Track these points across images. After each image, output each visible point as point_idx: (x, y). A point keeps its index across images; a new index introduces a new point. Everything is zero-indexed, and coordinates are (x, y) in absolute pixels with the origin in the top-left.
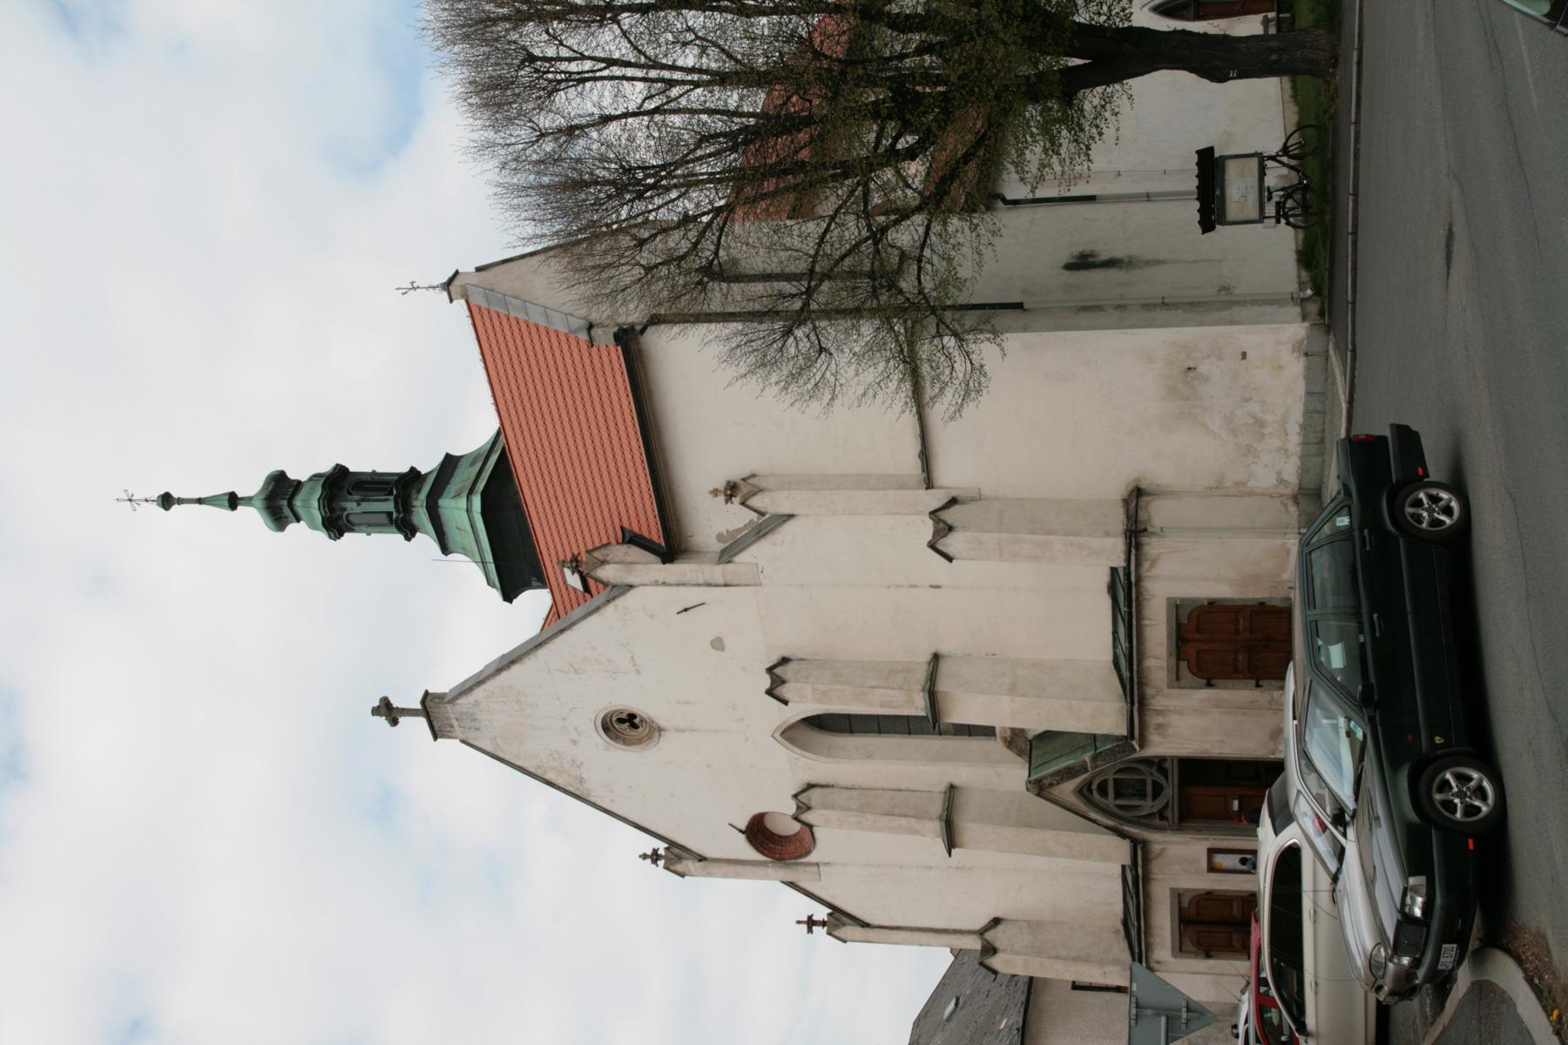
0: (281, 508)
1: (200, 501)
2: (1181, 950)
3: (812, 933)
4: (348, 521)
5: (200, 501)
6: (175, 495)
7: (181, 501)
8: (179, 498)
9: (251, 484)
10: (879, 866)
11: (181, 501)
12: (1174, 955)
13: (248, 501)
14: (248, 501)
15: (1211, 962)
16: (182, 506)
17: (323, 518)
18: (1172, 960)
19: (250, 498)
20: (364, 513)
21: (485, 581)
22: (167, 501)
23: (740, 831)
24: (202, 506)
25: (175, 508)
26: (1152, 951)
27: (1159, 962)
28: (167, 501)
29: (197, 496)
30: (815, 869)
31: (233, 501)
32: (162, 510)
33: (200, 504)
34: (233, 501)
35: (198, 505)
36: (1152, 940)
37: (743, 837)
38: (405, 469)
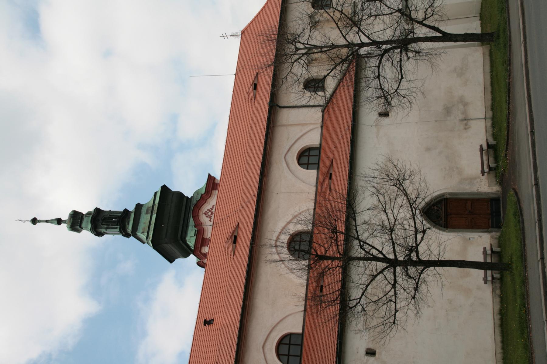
1: (47, 221)
5: (47, 221)
6: (38, 219)
7: (40, 221)
8: (39, 220)
9: (65, 216)
11: (40, 221)
13: (65, 222)
14: (65, 222)
16: (40, 223)
19: (66, 220)
22: (34, 221)
24: (48, 223)
25: (38, 224)
28: (34, 221)
29: (46, 219)
31: (59, 221)
32: (32, 225)
33: (47, 223)
34: (59, 221)
35: (46, 223)
38: (122, 210)
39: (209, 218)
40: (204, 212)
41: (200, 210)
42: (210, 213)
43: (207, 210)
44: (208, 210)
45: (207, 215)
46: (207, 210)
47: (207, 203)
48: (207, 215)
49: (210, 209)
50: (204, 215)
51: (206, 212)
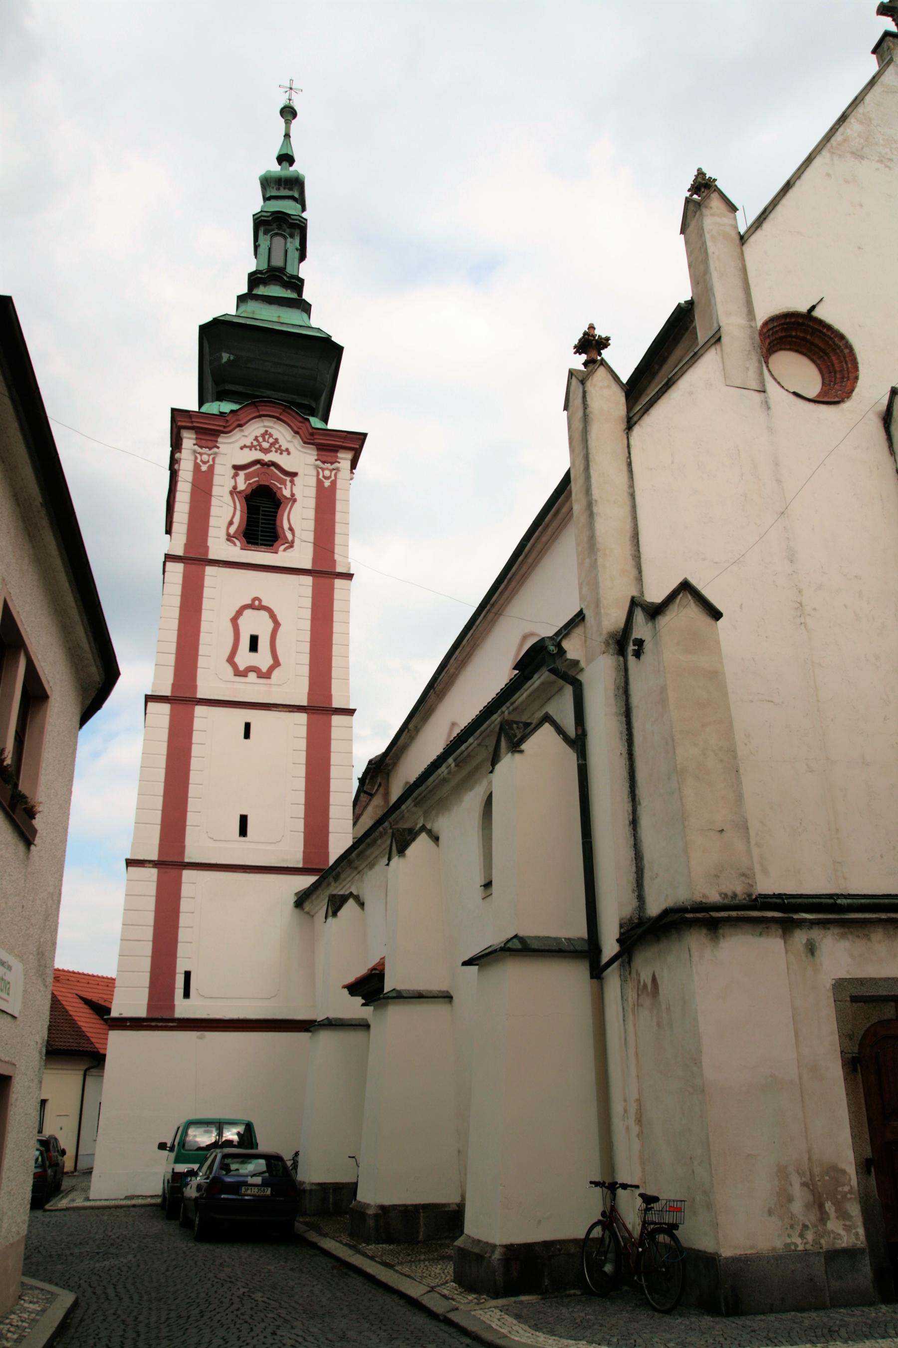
0: (291, 189)
2: (854, 999)
3: (608, 339)
4: (281, 235)
6: (294, 122)
10: (779, 481)
12: (840, 985)
15: (835, 1071)
17: (289, 215)
18: (826, 981)
20: (286, 251)
21: (228, 313)
22: (289, 113)
23: (813, 308)
24: (283, 138)
26: (843, 936)
27: (811, 949)
30: (755, 385)
31: (286, 158)
33: (284, 136)
34: (286, 158)
35: (284, 134)
36: (878, 935)
37: (803, 308)
39: (252, 443)
40: (270, 430)
41: (275, 420)
42: (265, 445)
43: (274, 437)
44: (276, 440)
45: (260, 439)
46: (274, 437)
47: (303, 447)
48: (260, 439)
49: (277, 446)
50: (262, 430)
51: (271, 435)
